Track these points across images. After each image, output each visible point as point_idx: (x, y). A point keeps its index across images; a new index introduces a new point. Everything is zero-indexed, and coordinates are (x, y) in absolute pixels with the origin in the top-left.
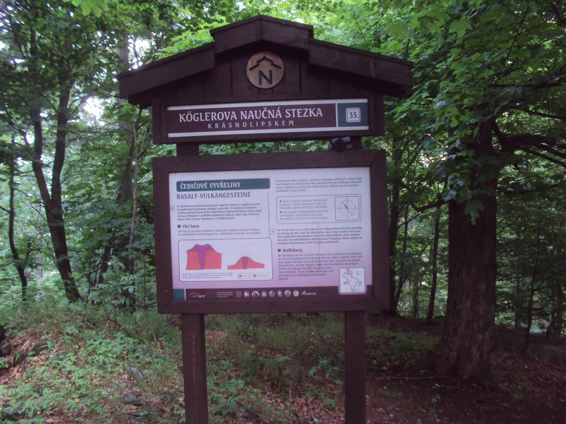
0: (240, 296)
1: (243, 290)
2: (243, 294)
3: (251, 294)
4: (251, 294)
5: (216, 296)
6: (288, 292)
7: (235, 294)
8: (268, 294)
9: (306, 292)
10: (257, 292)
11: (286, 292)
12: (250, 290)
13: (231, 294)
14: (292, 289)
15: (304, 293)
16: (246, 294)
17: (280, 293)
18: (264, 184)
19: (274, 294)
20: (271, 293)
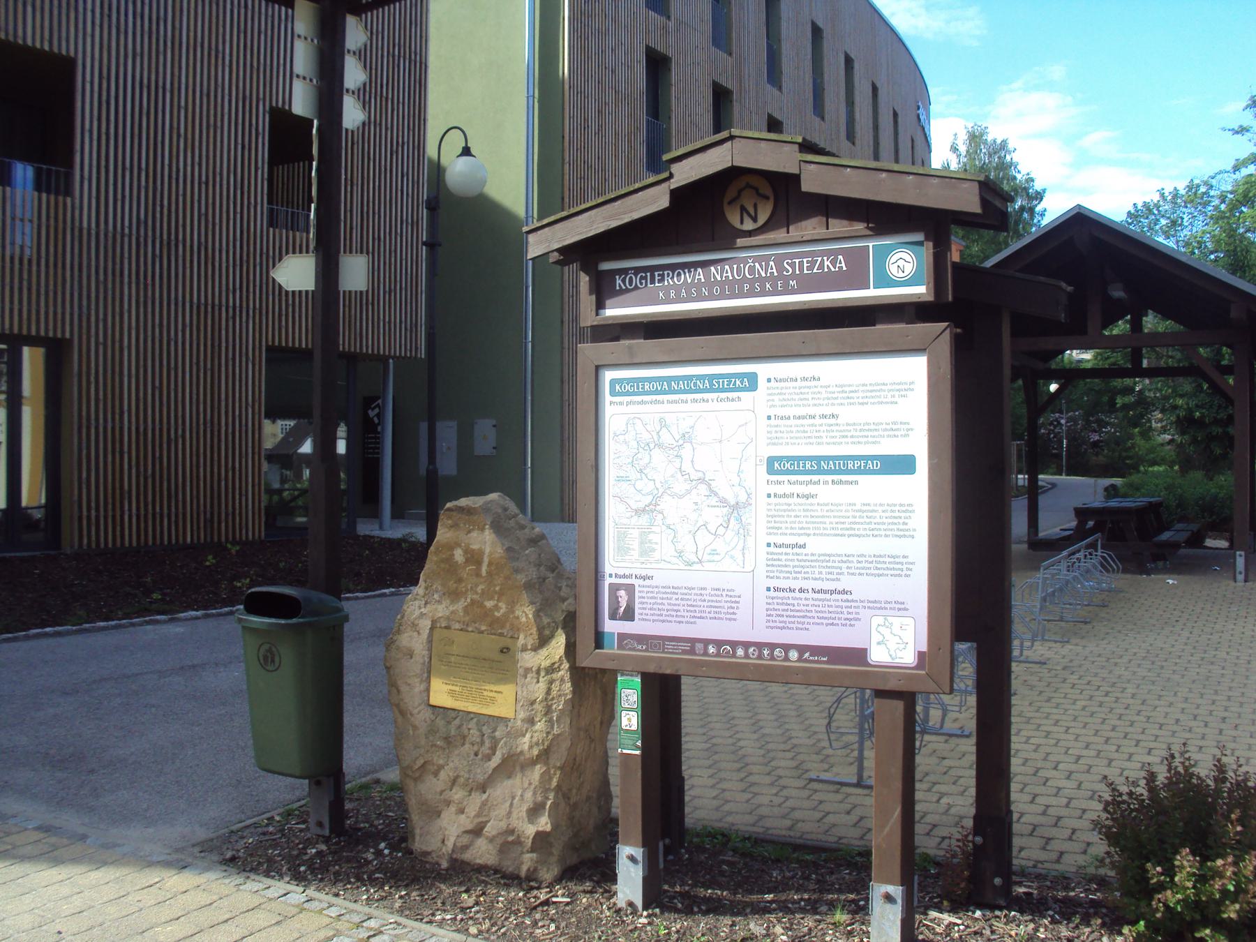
1: (706, 642)
2: (706, 648)
11: (777, 652)
12: (719, 643)
13: (687, 646)
14: (787, 648)
15: (807, 655)
16: (711, 650)
19: (756, 653)
20: (751, 650)
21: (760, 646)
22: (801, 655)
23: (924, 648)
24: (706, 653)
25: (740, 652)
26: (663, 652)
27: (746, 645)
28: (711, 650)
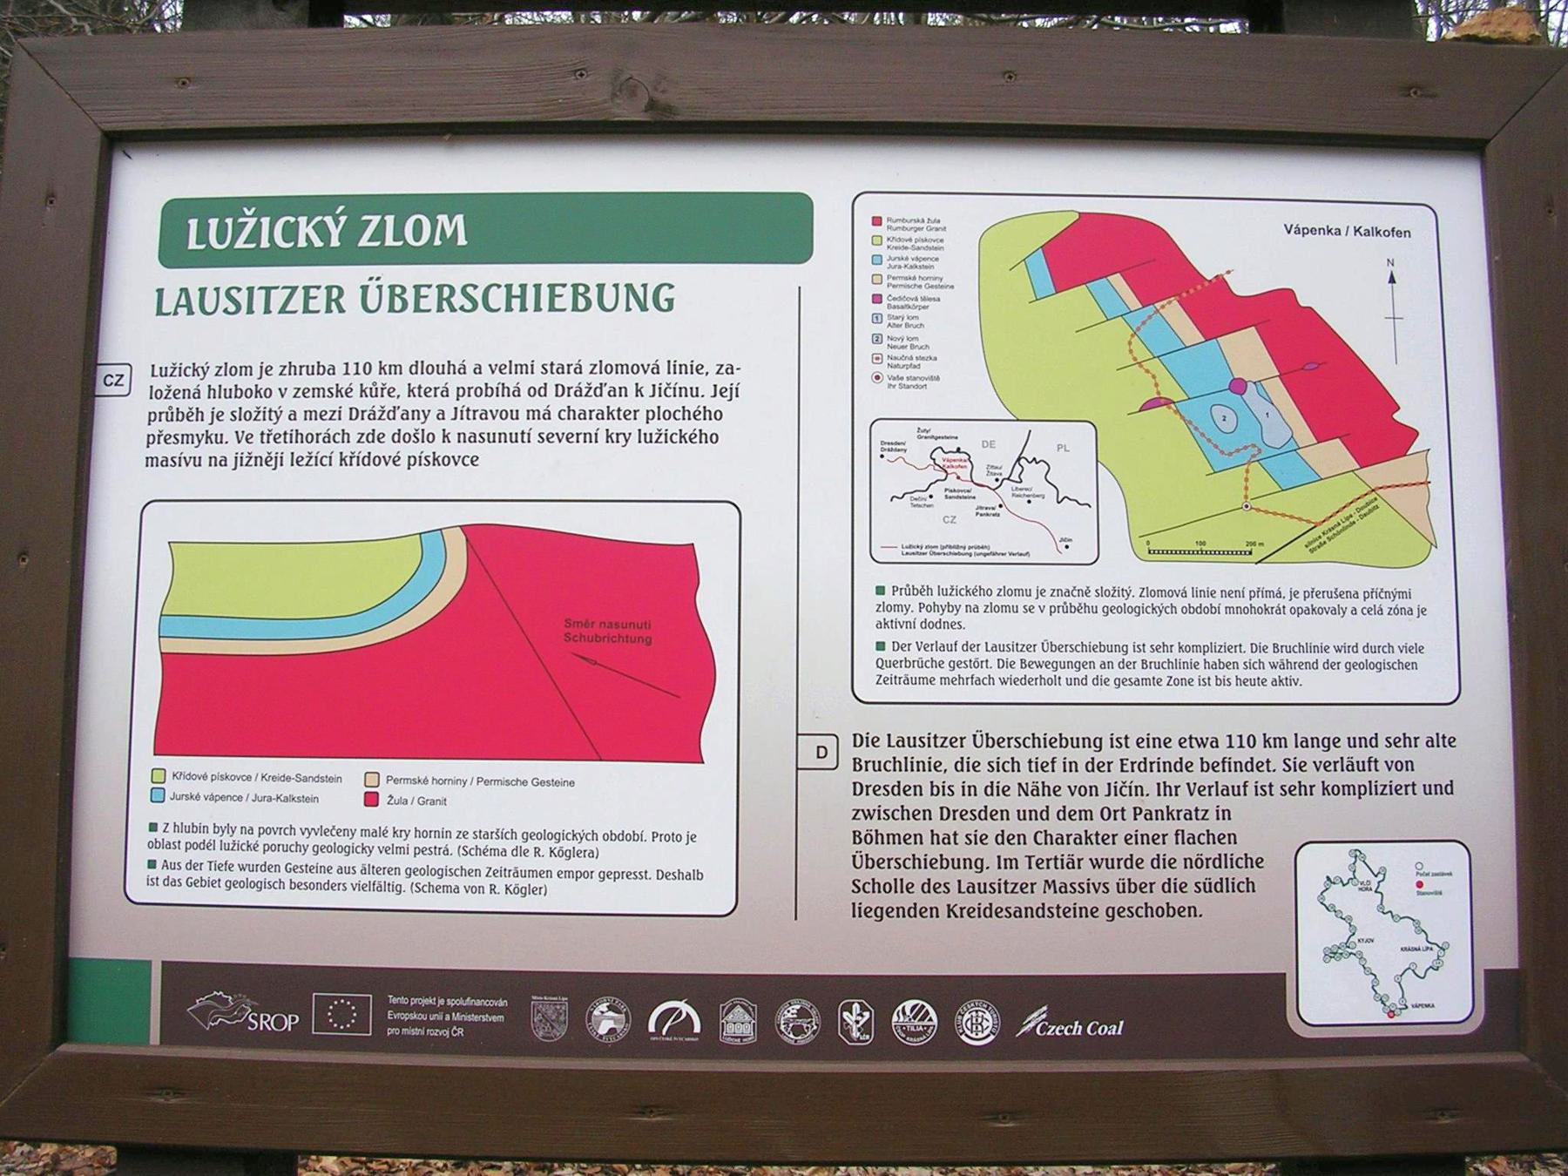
0: (561, 1031)
1: (582, 989)
2: (580, 1018)
3: (638, 1019)
4: (638, 1019)
5: (382, 1024)
6: (919, 1013)
7: (519, 1013)
8: (766, 1024)
9: (1052, 1019)
10: (685, 1008)
11: (904, 1014)
12: (638, 991)
13: (490, 1012)
14: (949, 992)
17: (854, 1018)
18: (778, 231)
19: (813, 1025)
20: (790, 1012)
21: (826, 992)
22: (1010, 1018)
23: (1508, 959)
24: (580, 1039)
25: (739, 1024)
26: (381, 1043)
27: (764, 992)
28: (606, 1020)
